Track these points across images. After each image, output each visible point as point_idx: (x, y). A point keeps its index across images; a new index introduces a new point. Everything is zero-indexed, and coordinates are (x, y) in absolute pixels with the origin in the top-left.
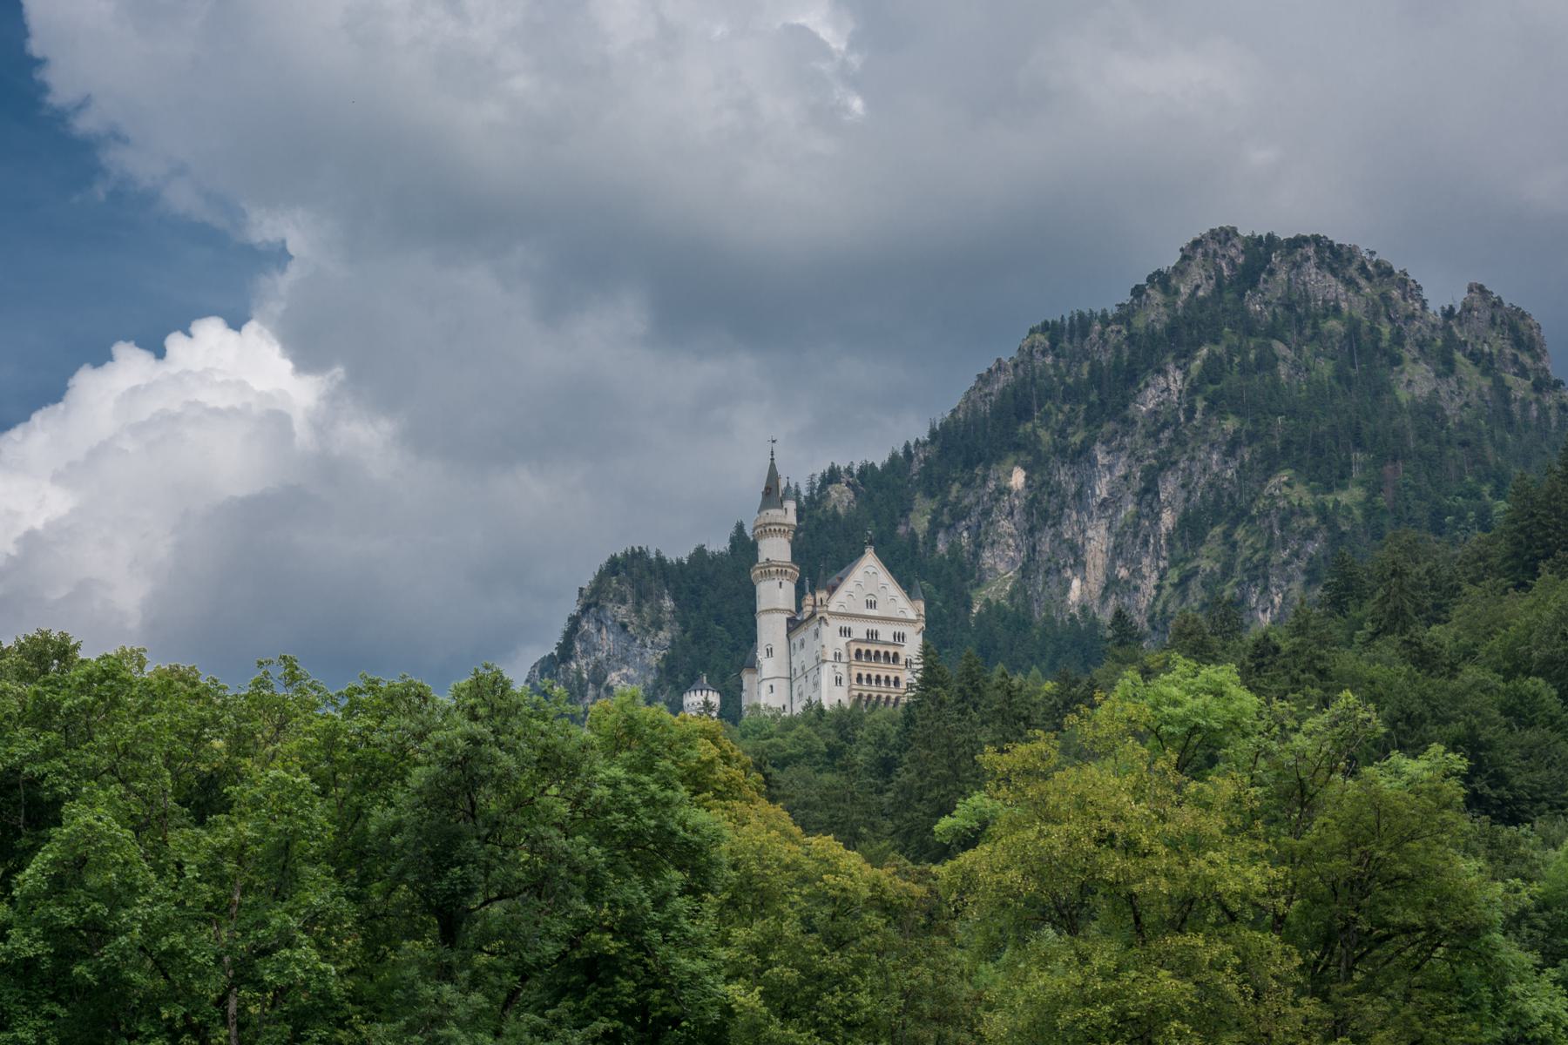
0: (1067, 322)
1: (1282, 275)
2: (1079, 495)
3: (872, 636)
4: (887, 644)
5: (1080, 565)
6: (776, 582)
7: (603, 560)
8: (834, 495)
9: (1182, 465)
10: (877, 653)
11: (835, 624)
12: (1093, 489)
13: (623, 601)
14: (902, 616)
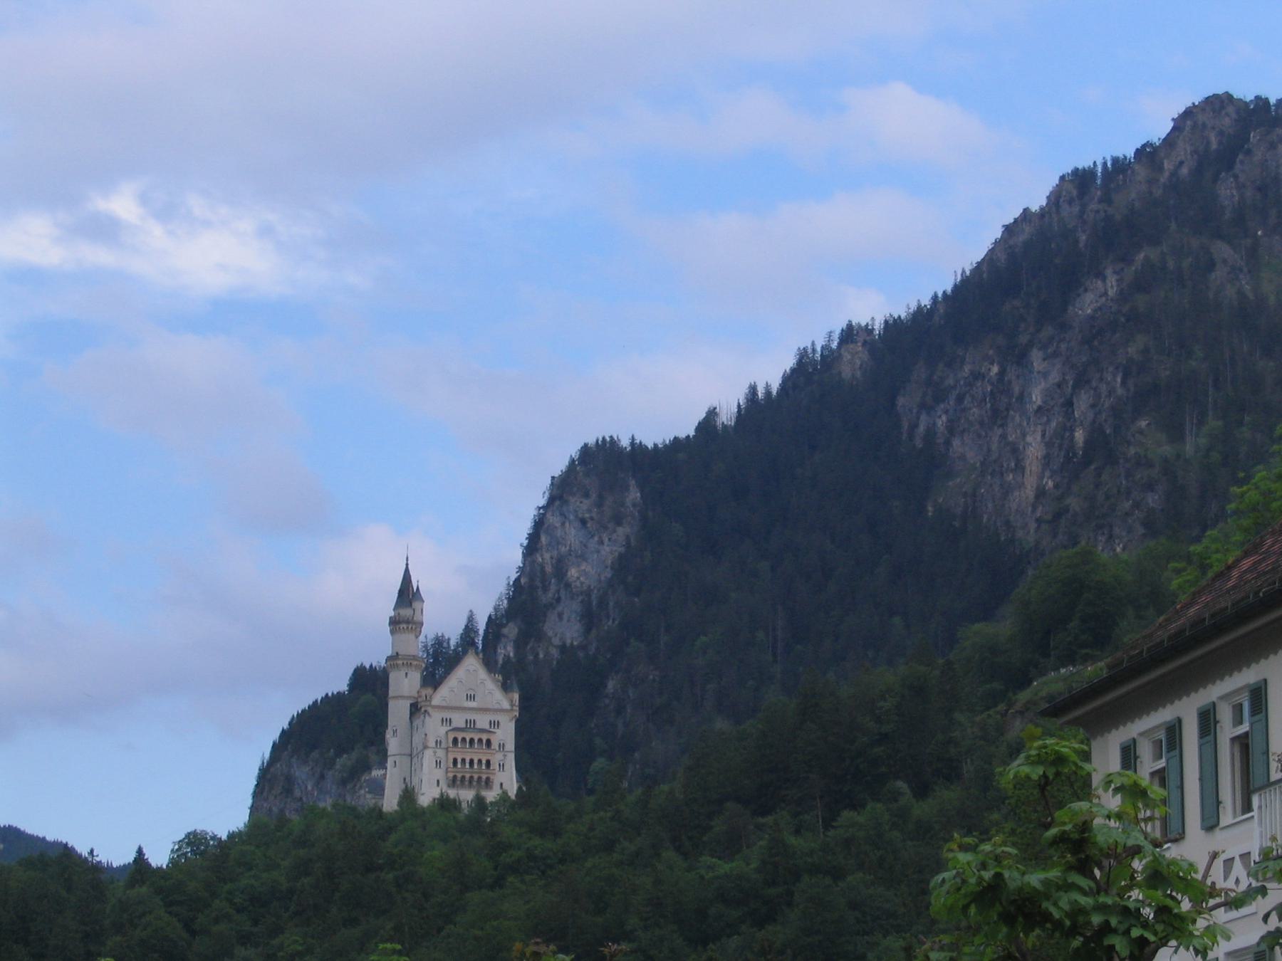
0: (1099, 169)
1: (1258, 156)
2: (1021, 398)
3: (470, 726)
4: (483, 731)
5: (1020, 468)
6: (403, 673)
7: (573, 450)
8: (847, 356)
9: (1094, 384)
10: (472, 740)
11: (436, 716)
12: (1030, 394)
13: (587, 495)
14: (496, 706)
